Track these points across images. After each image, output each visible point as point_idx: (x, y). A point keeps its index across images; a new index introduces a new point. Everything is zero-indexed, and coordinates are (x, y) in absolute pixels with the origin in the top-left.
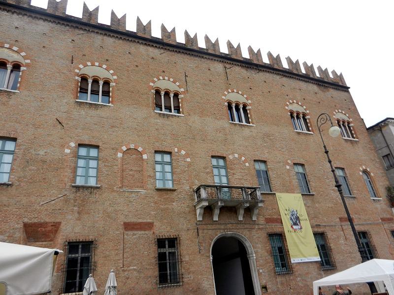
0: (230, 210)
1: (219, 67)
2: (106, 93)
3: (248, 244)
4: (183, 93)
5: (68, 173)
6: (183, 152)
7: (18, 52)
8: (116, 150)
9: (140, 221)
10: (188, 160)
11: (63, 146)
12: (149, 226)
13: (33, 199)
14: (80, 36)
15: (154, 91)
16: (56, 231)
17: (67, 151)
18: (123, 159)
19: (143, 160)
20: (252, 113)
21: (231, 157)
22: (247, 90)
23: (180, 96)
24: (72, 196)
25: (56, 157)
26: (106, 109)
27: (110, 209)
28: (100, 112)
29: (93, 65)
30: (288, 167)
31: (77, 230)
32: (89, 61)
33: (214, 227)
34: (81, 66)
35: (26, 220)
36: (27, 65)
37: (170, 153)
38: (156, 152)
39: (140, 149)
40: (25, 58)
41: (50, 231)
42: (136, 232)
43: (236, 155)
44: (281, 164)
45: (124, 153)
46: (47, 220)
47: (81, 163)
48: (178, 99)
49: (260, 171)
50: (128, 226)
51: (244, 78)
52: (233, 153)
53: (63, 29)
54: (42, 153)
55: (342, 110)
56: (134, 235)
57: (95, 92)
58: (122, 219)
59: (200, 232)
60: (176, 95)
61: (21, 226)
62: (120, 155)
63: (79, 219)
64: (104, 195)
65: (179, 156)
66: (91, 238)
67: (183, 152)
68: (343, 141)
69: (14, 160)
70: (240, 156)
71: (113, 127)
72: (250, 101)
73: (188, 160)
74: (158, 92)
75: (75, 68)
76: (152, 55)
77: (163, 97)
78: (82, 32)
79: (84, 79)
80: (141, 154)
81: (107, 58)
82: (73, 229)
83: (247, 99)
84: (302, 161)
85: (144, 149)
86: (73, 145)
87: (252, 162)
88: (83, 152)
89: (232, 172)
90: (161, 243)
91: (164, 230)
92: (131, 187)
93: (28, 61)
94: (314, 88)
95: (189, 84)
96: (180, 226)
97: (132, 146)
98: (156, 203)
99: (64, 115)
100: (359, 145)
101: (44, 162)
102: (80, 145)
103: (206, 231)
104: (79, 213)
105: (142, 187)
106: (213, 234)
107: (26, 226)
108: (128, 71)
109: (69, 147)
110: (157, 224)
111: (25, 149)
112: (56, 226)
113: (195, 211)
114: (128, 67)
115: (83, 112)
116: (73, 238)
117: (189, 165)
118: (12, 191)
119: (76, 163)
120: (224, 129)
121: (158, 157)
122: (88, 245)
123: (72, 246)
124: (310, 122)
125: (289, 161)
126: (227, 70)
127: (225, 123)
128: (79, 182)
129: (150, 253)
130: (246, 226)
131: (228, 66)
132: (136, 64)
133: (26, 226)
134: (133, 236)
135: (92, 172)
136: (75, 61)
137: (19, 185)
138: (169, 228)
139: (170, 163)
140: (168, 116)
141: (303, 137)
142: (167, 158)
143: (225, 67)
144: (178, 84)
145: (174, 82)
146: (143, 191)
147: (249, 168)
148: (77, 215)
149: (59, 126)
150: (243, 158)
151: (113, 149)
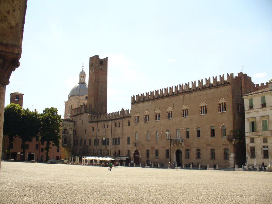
1: (181, 97)
6: (171, 130)
8: (161, 131)
21: (181, 129)
30: (195, 129)
50: (162, 147)
52: (181, 128)
55: (223, 98)
66: (158, 149)
67: (171, 130)
80: (164, 131)
82: (156, 148)
84: (200, 126)
107: (152, 147)
112: (154, 147)
116: (156, 149)
125: (196, 127)
127: (181, 118)
131: (184, 95)
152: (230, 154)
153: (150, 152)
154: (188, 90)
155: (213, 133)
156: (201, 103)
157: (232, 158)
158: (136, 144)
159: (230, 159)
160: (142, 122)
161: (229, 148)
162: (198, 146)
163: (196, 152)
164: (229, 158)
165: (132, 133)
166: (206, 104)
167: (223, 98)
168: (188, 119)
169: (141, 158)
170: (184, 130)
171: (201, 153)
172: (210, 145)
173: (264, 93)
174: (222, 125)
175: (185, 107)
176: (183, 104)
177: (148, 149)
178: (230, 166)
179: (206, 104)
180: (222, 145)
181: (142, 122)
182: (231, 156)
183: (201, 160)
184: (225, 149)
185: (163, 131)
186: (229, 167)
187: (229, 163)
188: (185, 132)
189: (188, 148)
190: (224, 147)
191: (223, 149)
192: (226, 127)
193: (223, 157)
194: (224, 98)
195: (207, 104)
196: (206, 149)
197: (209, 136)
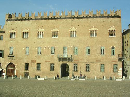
1: (70, 20)
4: (59, 31)
6: (57, 47)
7: (28, 29)
8: (44, 47)
12: (49, 61)
27: (43, 58)
31: (38, 61)
37: (54, 47)
39: (48, 47)
44: (82, 47)
50: (46, 61)
58: (45, 60)
62: (45, 48)
67: (57, 47)
70: (71, 46)
72: (77, 30)
80: (48, 48)
82: (38, 61)
83: (77, 29)
84: (89, 46)
90: (51, 64)
92: (46, 54)
106: (62, 63)
110: (51, 61)
112: (35, 61)
120: (68, 39)
123: (38, 64)
125: (85, 46)
127: (69, 38)
129: (49, 66)
131: (73, 19)
132: (48, 26)
134: (46, 63)
144: (58, 29)
146: (48, 55)
153: (30, 65)
154: (52, 17)
155: (102, 52)
157: (120, 71)
160: (19, 38)
163: (85, 66)
164: (118, 71)
166: (97, 29)
169: (17, 71)
174: (112, 46)
175: (73, 30)
176: (72, 26)
177: (27, 62)
178: (119, 77)
179: (97, 29)
181: (19, 38)
182: (119, 70)
186: (118, 78)
187: (118, 75)
190: (113, 63)
195: (97, 29)
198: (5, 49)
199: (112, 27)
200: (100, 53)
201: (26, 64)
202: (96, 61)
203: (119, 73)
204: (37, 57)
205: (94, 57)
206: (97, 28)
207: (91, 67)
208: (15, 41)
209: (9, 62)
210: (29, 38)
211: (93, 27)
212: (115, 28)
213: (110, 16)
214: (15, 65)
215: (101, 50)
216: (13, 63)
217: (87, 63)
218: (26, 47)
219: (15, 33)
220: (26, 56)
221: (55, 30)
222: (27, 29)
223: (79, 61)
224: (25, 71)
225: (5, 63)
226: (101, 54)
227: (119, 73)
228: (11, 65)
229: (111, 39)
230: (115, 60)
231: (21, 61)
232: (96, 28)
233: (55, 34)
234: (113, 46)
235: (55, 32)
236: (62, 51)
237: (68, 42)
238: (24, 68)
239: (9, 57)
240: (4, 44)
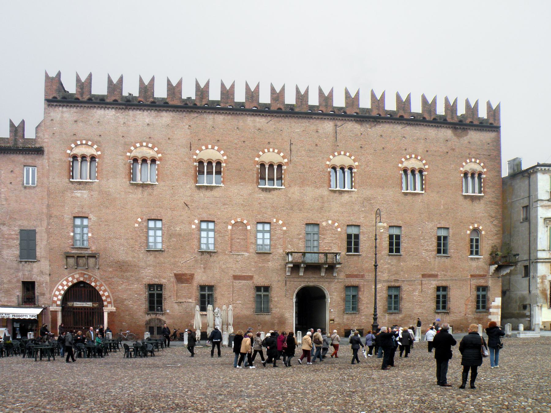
0: (313, 268)
1: (328, 126)
2: (218, 173)
3: (327, 292)
4: (287, 164)
5: (196, 242)
6: (281, 222)
7: (152, 148)
8: (227, 223)
9: (244, 274)
10: (285, 228)
11: (190, 223)
12: (251, 278)
13: (177, 260)
14: (195, 120)
15: (258, 166)
16: (192, 279)
17: (194, 227)
18: (231, 230)
19: (247, 230)
20: (357, 177)
21: (324, 224)
22: (356, 150)
23: (284, 167)
24: (199, 258)
25: (187, 232)
26: (218, 189)
27: (224, 267)
28: (215, 193)
29: (207, 148)
31: (204, 278)
32: (203, 145)
33: (299, 280)
34: (198, 152)
35: (175, 272)
36: (160, 159)
38: (258, 223)
39: (245, 222)
40: (158, 152)
41: (188, 279)
42: (241, 281)
43: (330, 222)
45: (233, 225)
46: (186, 272)
47: (204, 234)
48: (282, 170)
49: (351, 235)
50: (236, 277)
51: (357, 135)
53: (181, 116)
54: (178, 229)
55: (476, 159)
56: (240, 283)
57: (210, 173)
58: (232, 273)
59: (288, 283)
60: (280, 166)
61: (173, 275)
62: (230, 227)
63: (204, 272)
64: (220, 257)
65: (278, 225)
66: (212, 284)
67: (281, 222)
68: (461, 199)
69: (163, 235)
70: (334, 222)
71: (224, 204)
72: (357, 164)
73: (285, 228)
74: (263, 165)
75: (193, 155)
76: (258, 125)
77: (267, 170)
78: (196, 115)
79: (201, 162)
80: (246, 225)
81: (217, 138)
82: (201, 278)
84: (400, 223)
85: (248, 221)
86: (196, 221)
87: (345, 228)
88: (204, 226)
89: (323, 237)
90: (258, 289)
91: (260, 281)
92: (238, 251)
93: (160, 155)
94: (448, 133)
95: (293, 153)
96: (273, 279)
97: (239, 220)
98: (256, 262)
99: (189, 198)
100: (482, 201)
101: (180, 235)
102: (202, 221)
103: (292, 283)
104: (204, 268)
105: (246, 251)
107: (176, 275)
108: (236, 148)
109: (194, 224)
110: (256, 277)
111: (168, 227)
112: (192, 276)
113: (286, 268)
114: (236, 144)
115: (202, 194)
116: (202, 283)
117: (285, 232)
118: (165, 254)
119: (200, 235)
120: (322, 197)
121: (260, 227)
122: (211, 288)
123: (202, 288)
124: (425, 180)
126: (338, 128)
128: (204, 247)
129: (251, 294)
130: (326, 280)
131: (339, 123)
132: (243, 139)
133: (176, 275)
135: (211, 241)
136: (192, 148)
137: (168, 251)
138: (264, 280)
139: (269, 232)
140: (269, 190)
141: (410, 198)
142: (267, 227)
143: (336, 126)
144: (282, 154)
145: (279, 153)
146: (246, 254)
147: (340, 232)
148: (203, 270)
149: (187, 208)
150: (336, 224)
151: (224, 223)
152: (491, 299)
155: (442, 246)
156: (406, 159)
157: (497, 307)
158: (78, 257)
159: (491, 310)
161: (490, 283)
162: (393, 278)
165: (50, 216)
166: (424, 165)
167: (476, 159)
168: (354, 196)
169: (110, 314)
170: (339, 230)
171: (404, 295)
172: (435, 276)
173: (545, 169)
174: (471, 227)
176: (335, 149)
177: (156, 281)
179: (424, 165)
180: (472, 276)
182: (493, 304)
183: (401, 316)
184: (478, 288)
185: (236, 222)
188: (345, 237)
189: (354, 282)
191: (474, 287)
192: (483, 233)
193: (472, 305)
194: (478, 161)
195: (427, 167)
196: (419, 287)
197: (434, 251)
198: (48, 224)
199: (473, 160)
200: (436, 248)
201: (150, 286)
202: (424, 276)
203: (494, 314)
204: (196, 261)
205: (416, 264)
206: (424, 162)
207: (404, 296)
208: (95, 194)
209: (70, 279)
210: (162, 184)
211: (413, 156)
212: (482, 164)
213: (468, 121)
214: (101, 293)
215: (439, 238)
216: (93, 284)
217: (393, 284)
218: (145, 217)
219: (93, 158)
220: (151, 258)
221: (271, 156)
222: (150, 145)
223: (363, 276)
224: (148, 318)
225: (53, 284)
226: (439, 251)
227: (494, 314)
228: (80, 290)
229: (468, 201)
230: (482, 273)
231: (128, 274)
232: (421, 160)
233: (269, 172)
234: (476, 226)
235: (271, 166)
236: (300, 239)
237: (322, 208)
238: (144, 305)
239: (71, 261)
240: (46, 202)
